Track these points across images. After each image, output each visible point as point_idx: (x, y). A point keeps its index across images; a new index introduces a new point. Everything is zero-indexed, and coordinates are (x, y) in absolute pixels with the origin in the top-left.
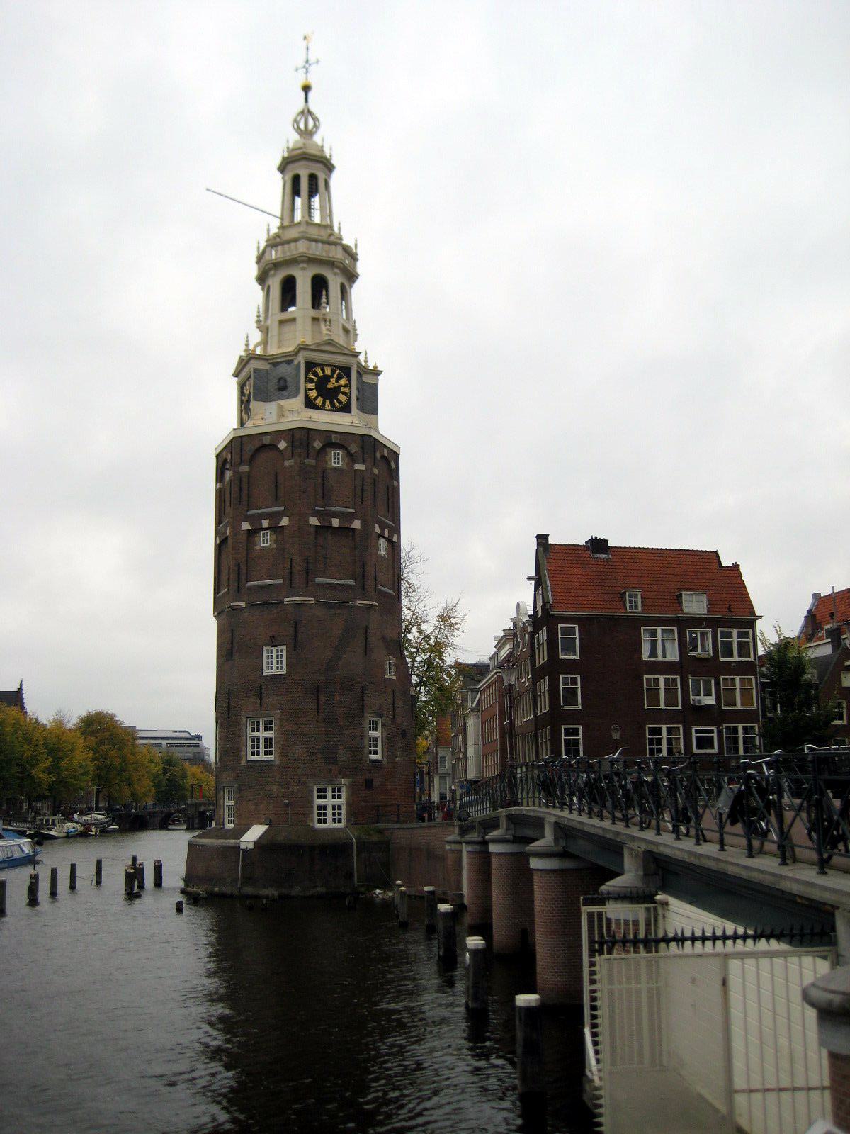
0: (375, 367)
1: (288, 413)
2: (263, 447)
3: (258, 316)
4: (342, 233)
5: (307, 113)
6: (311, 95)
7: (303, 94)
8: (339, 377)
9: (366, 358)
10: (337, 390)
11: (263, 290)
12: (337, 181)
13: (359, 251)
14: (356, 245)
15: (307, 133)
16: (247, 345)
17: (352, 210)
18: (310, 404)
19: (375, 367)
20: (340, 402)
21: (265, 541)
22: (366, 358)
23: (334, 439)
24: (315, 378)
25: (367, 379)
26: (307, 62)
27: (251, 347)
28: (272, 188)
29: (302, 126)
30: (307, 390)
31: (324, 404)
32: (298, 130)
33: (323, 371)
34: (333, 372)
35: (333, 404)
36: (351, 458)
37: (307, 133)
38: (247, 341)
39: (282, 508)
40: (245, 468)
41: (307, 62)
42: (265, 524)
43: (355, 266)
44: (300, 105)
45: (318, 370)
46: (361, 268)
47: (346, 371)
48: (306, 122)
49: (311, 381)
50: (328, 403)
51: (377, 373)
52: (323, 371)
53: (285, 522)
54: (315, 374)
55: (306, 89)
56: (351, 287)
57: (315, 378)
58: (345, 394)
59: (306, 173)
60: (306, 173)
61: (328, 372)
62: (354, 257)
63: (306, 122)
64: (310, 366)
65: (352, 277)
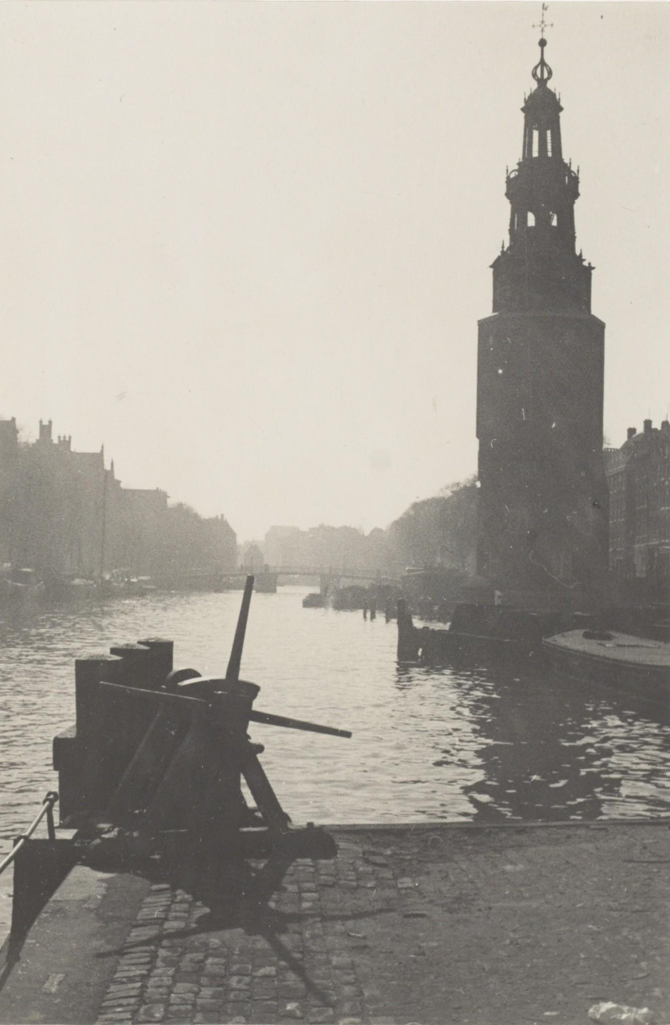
0: (589, 264)
4: (566, 158)
5: (542, 63)
6: (545, 48)
7: (539, 48)
12: (564, 118)
13: (580, 176)
15: (542, 82)
16: (503, 247)
19: (589, 264)
26: (543, 22)
37: (542, 82)
41: (543, 22)
46: (581, 189)
48: (542, 72)
55: (543, 43)
63: (542, 72)
65: (576, 195)
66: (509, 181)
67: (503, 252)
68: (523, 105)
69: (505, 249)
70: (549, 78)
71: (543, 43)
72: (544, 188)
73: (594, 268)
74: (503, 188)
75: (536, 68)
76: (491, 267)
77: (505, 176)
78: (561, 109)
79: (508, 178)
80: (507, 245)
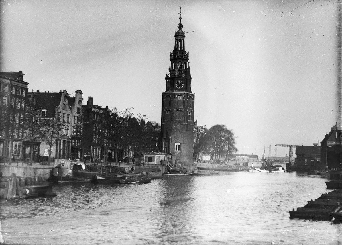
2: (167, 96)
3: (169, 68)
6: (181, 20)
7: (180, 20)
12: (185, 39)
16: (167, 74)
23: (180, 95)
26: (181, 12)
27: (168, 74)
28: (172, 40)
41: (181, 12)
44: (179, 23)
46: (189, 58)
48: (180, 26)
55: (180, 19)
59: (180, 36)
60: (180, 36)
62: (188, 56)
63: (180, 26)
65: (187, 60)
69: (168, 74)
71: (180, 19)
72: (179, 57)
78: (185, 36)
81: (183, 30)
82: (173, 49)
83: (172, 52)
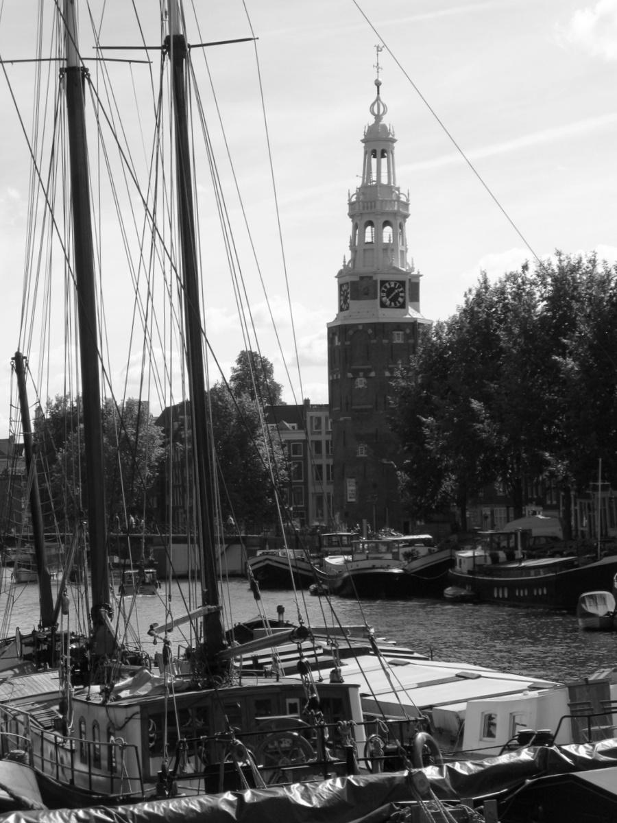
1: (371, 312)
8: (399, 287)
9: (413, 262)
10: (397, 296)
11: (353, 221)
14: (408, 194)
15: (378, 118)
16: (345, 262)
17: (407, 173)
18: (383, 305)
19: (419, 272)
20: (399, 302)
21: (361, 383)
22: (413, 262)
24: (386, 290)
25: (413, 281)
29: (376, 112)
30: (382, 297)
31: (390, 304)
32: (373, 113)
33: (389, 284)
34: (395, 284)
35: (395, 304)
36: (407, 337)
37: (378, 118)
38: (345, 259)
39: (370, 367)
40: (348, 343)
42: (361, 374)
43: (407, 209)
45: (387, 285)
46: (412, 210)
47: (402, 284)
49: (383, 292)
50: (393, 304)
51: (418, 276)
52: (389, 284)
53: (373, 374)
54: (386, 287)
55: (378, 84)
56: (405, 221)
57: (386, 290)
58: (402, 297)
59: (378, 144)
60: (378, 144)
61: (393, 286)
62: (406, 205)
64: (383, 283)
66: (351, 204)
67: (344, 266)
68: (363, 137)
69: (346, 264)
70: (384, 113)
71: (378, 84)
73: (422, 276)
74: (346, 209)
75: (373, 105)
76: (336, 277)
77: (347, 199)
78: (394, 141)
79: (350, 200)
80: (349, 258)
81: (385, 121)
82: (358, 183)
83: (353, 191)
